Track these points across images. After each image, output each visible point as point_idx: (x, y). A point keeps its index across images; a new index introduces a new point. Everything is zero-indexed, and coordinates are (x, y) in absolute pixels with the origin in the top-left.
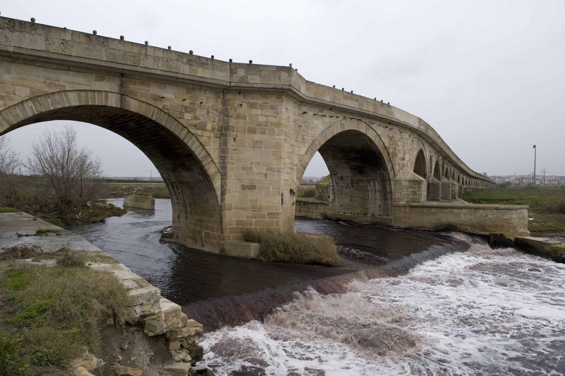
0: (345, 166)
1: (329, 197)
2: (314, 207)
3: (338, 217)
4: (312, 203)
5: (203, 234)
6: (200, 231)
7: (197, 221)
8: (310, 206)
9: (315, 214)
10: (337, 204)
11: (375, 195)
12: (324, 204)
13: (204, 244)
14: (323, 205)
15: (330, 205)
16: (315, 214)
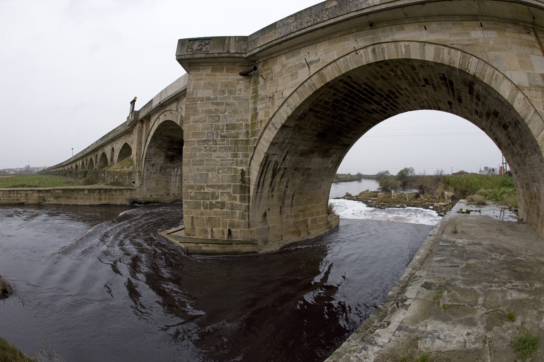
0: (163, 154)
1: (134, 182)
2: (118, 193)
3: (147, 200)
4: (116, 190)
5: (309, 222)
6: (305, 220)
7: (299, 211)
8: (114, 193)
9: (120, 200)
10: (144, 188)
11: (176, 178)
12: (131, 189)
13: (310, 231)
14: (129, 191)
15: (138, 190)
16: (120, 200)
